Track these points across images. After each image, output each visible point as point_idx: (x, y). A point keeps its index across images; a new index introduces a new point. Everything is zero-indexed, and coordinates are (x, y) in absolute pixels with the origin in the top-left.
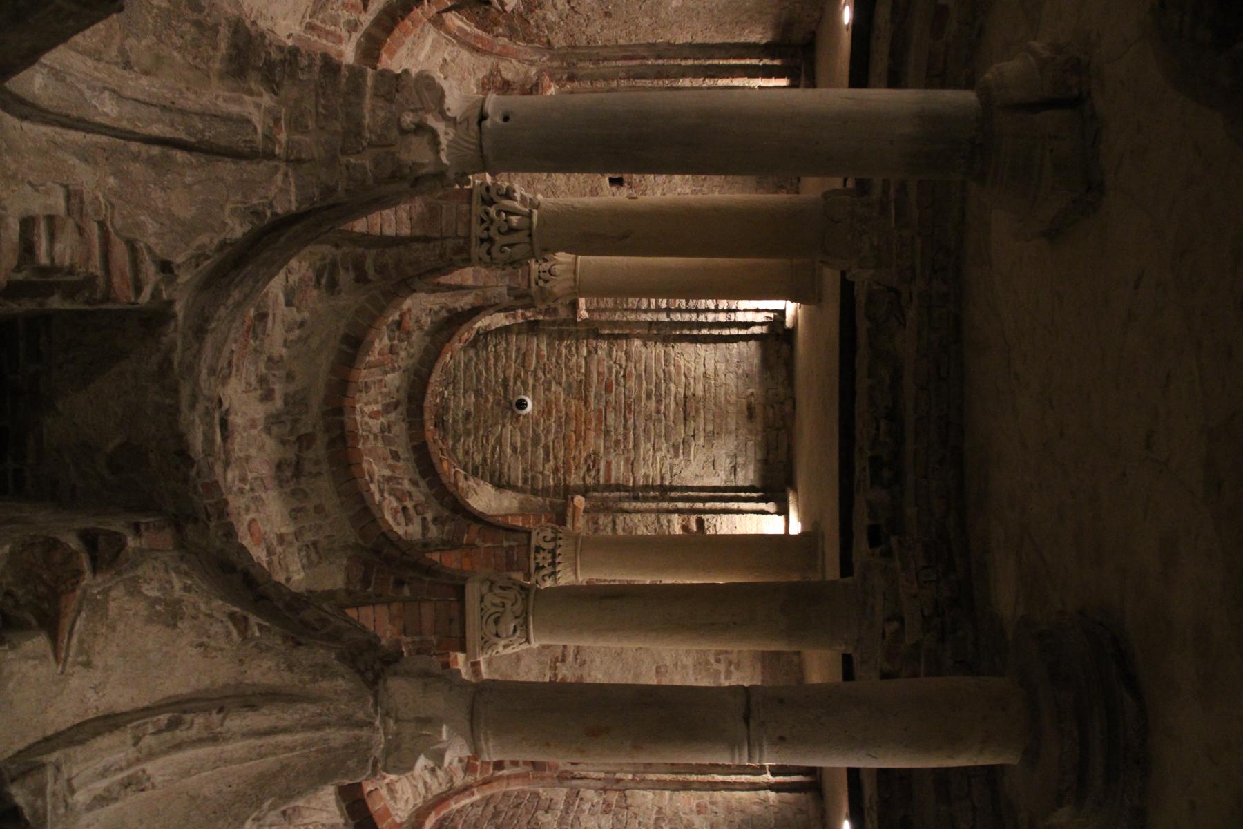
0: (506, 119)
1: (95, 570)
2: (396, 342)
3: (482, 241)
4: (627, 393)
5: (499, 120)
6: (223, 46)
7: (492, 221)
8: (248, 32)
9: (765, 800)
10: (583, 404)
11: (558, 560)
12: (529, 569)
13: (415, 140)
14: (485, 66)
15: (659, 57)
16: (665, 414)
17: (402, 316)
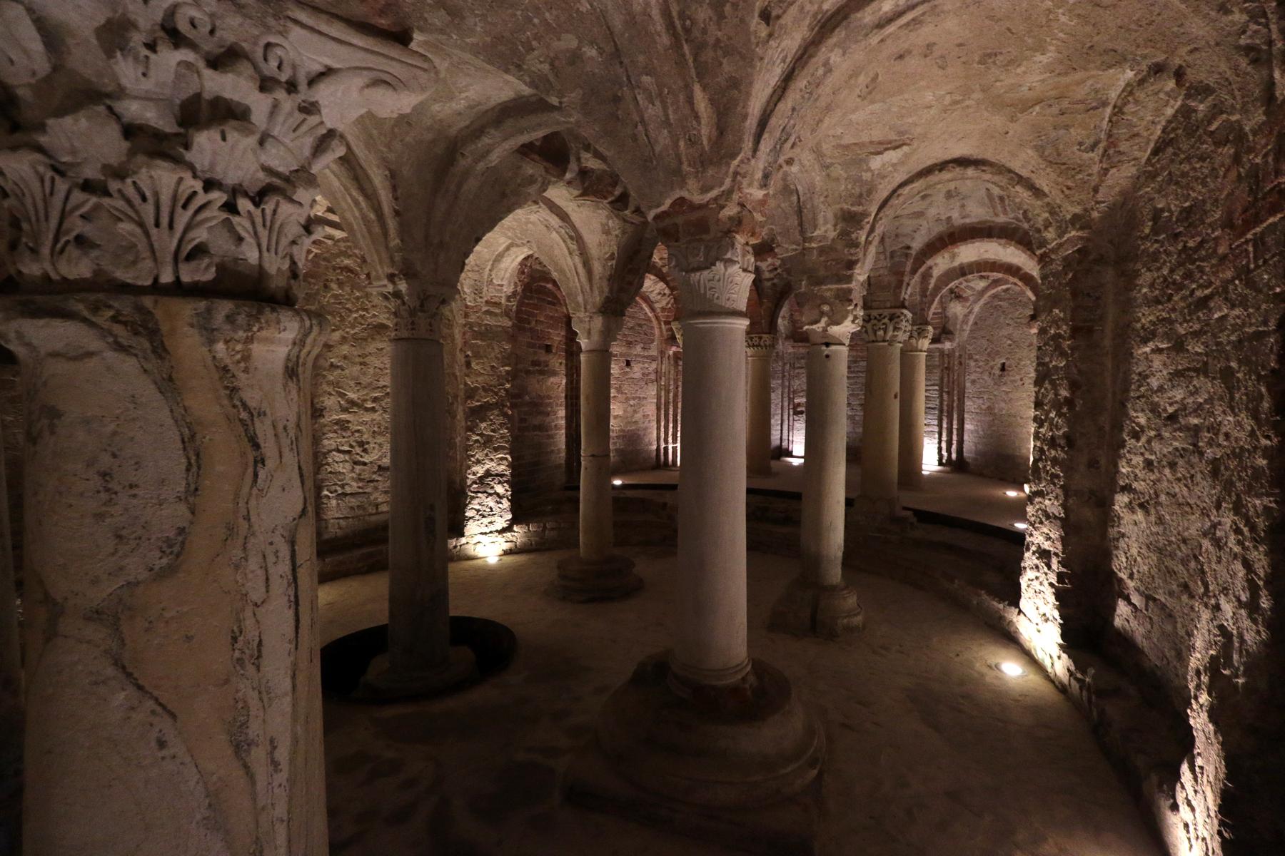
0: (827, 356)
1: (611, 203)
3: (869, 316)
5: (826, 353)
6: (854, 209)
7: (879, 321)
8: (862, 221)
9: (651, 444)
13: (816, 312)
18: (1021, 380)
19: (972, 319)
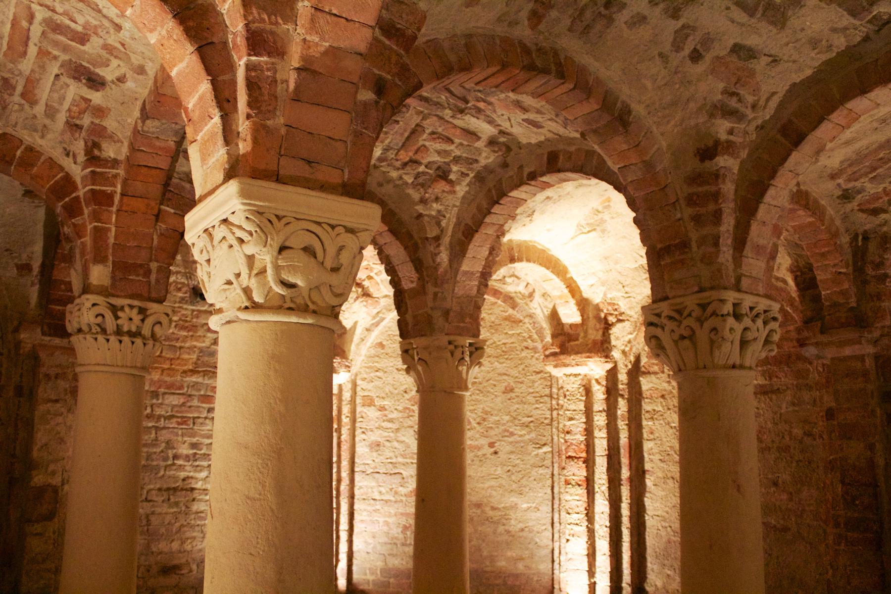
2: (422, 168)
4: (200, 420)
10: (191, 367)
11: (126, 339)
12: (113, 296)
14: (630, 308)
15: (631, 480)
16: (174, 464)
17: (451, 182)
18: (491, 445)
19: (374, 337)
